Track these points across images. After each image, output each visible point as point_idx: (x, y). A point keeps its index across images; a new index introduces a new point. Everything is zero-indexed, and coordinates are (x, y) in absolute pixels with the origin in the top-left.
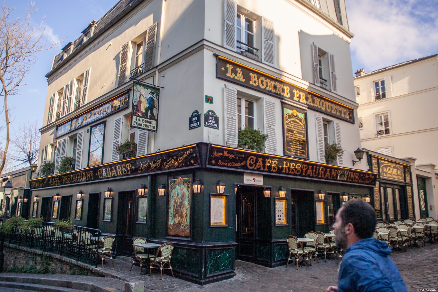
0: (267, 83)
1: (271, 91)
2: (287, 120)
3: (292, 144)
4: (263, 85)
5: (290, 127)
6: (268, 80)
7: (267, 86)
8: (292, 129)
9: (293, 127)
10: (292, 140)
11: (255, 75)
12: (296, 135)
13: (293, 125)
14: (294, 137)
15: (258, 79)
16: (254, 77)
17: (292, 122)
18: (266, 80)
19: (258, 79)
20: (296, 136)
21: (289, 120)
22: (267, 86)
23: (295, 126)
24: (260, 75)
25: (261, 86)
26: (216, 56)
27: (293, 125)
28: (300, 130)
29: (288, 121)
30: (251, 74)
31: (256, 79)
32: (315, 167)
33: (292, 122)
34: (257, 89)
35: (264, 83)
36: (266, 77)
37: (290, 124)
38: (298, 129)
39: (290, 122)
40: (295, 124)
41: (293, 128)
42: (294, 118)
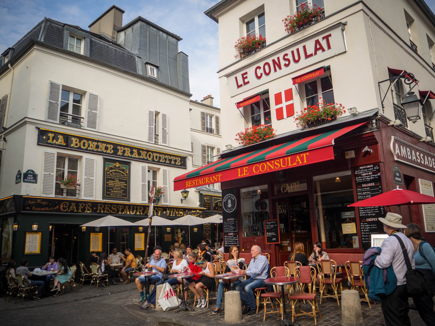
0: (89, 144)
1: (93, 151)
2: (107, 171)
3: (112, 190)
4: (84, 146)
5: (110, 177)
6: (90, 142)
7: (89, 146)
8: (113, 178)
9: (114, 176)
10: (112, 186)
11: (76, 139)
12: (117, 182)
13: (114, 174)
14: (115, 184)
15: (80, 142)
16: (76, 141)
17: (113, 173)
18: (88, 142)
19: (80, 142)
20: (117, 183)
21: (110, 171)
22: (89, 146)
23: (117, 175)
24: (81, 139)
25: (82, 147)
26: (38, 129)
27: (114, 174)
28: (121, 178)
29: (109, 172)
30: (73, 139)
31: (78, 142)
32: (135, 207)
33: (113, 173)
34: (79, 149)
35: (86, 145)
36: (88, 140)
37: (111, 174)
38: (119, 178)
39: (111, 173)
40: (116, 174)
41: (114, 177)
42: (116, 169)
